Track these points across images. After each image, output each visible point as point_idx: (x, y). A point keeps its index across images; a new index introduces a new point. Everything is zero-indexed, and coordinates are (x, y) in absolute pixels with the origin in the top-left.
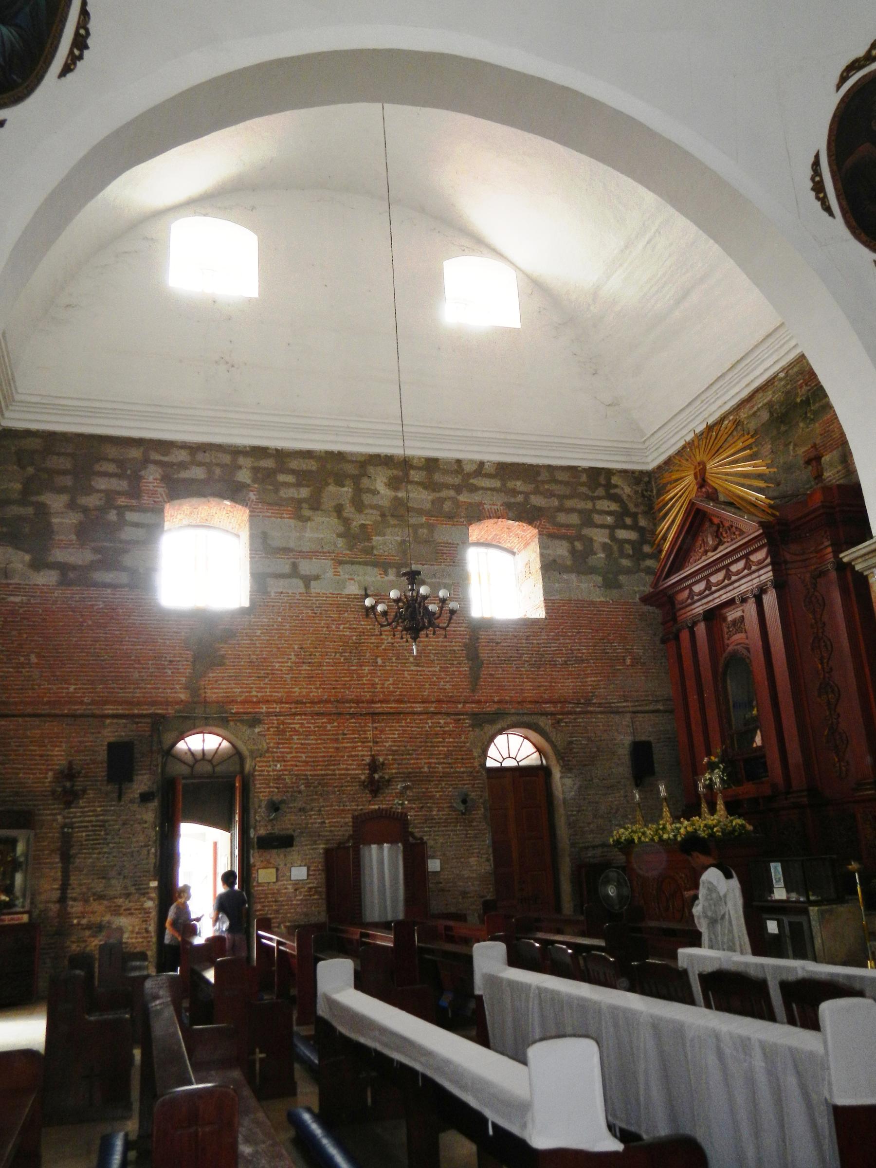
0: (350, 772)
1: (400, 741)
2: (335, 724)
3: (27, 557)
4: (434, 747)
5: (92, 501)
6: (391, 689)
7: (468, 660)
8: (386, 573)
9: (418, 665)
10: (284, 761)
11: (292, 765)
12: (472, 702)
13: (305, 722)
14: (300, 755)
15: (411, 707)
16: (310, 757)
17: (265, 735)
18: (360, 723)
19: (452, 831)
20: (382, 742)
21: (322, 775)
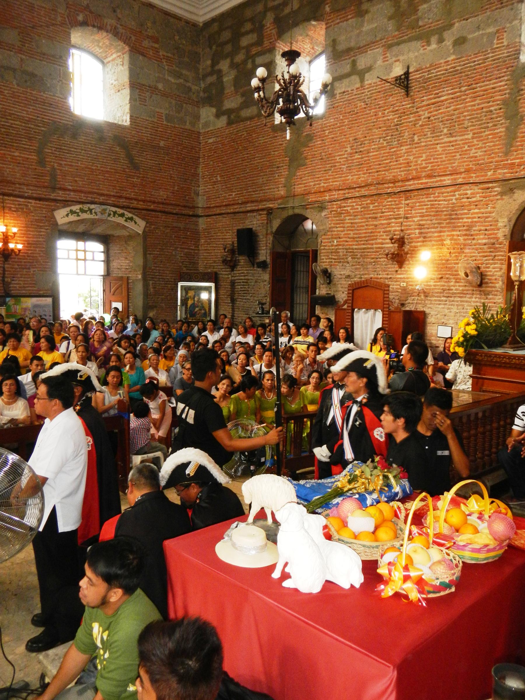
0: (384, 246)
1: (427, 216)
2: (376, 204)
3: (214, 110)
4: (459, 219)
5: (240, 58)
6: (424, 165)
7: (507, 118)
8: (429, 43)
9: (451, 135)
10: (339, 238)
11: (344, 241)
12: (504, 167)
13: (354, 204)
14: (349, 232)
15: (441, 181)
16: (357, 234)
17: (328, 218)
18: (395, 201)
19: (467, 302)
20: (411, 217)
21: (364, 249)
